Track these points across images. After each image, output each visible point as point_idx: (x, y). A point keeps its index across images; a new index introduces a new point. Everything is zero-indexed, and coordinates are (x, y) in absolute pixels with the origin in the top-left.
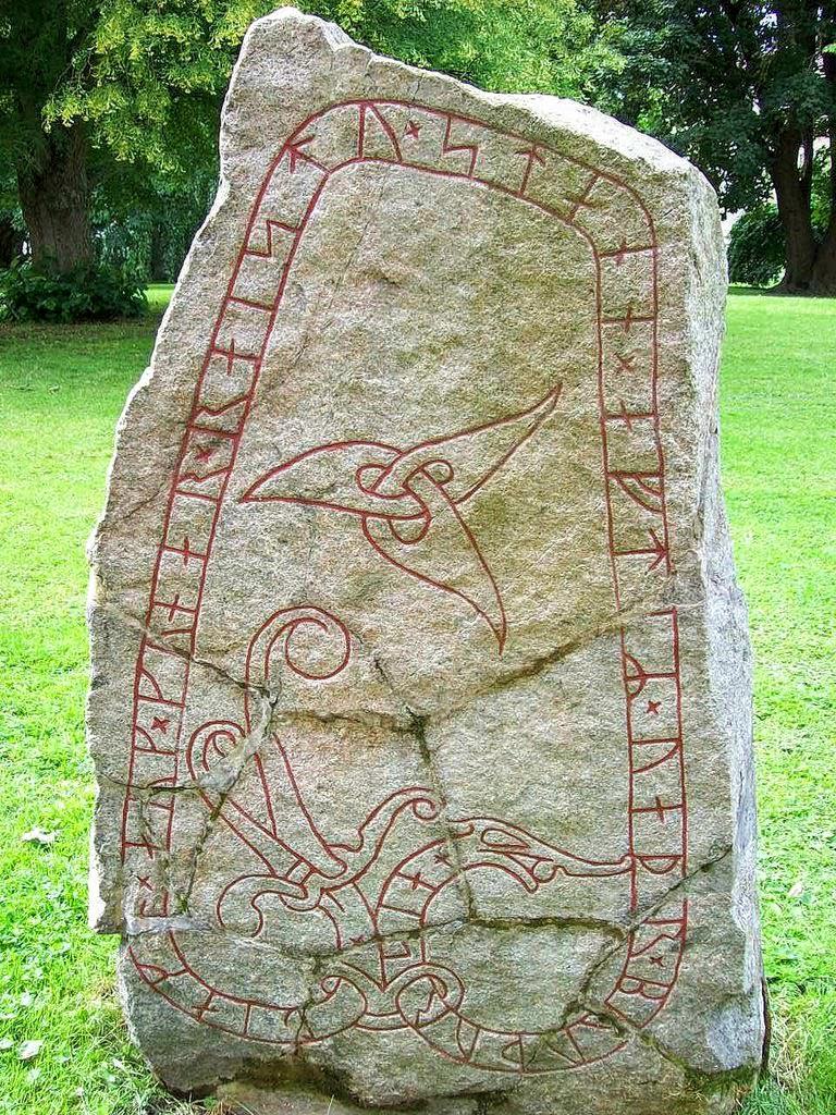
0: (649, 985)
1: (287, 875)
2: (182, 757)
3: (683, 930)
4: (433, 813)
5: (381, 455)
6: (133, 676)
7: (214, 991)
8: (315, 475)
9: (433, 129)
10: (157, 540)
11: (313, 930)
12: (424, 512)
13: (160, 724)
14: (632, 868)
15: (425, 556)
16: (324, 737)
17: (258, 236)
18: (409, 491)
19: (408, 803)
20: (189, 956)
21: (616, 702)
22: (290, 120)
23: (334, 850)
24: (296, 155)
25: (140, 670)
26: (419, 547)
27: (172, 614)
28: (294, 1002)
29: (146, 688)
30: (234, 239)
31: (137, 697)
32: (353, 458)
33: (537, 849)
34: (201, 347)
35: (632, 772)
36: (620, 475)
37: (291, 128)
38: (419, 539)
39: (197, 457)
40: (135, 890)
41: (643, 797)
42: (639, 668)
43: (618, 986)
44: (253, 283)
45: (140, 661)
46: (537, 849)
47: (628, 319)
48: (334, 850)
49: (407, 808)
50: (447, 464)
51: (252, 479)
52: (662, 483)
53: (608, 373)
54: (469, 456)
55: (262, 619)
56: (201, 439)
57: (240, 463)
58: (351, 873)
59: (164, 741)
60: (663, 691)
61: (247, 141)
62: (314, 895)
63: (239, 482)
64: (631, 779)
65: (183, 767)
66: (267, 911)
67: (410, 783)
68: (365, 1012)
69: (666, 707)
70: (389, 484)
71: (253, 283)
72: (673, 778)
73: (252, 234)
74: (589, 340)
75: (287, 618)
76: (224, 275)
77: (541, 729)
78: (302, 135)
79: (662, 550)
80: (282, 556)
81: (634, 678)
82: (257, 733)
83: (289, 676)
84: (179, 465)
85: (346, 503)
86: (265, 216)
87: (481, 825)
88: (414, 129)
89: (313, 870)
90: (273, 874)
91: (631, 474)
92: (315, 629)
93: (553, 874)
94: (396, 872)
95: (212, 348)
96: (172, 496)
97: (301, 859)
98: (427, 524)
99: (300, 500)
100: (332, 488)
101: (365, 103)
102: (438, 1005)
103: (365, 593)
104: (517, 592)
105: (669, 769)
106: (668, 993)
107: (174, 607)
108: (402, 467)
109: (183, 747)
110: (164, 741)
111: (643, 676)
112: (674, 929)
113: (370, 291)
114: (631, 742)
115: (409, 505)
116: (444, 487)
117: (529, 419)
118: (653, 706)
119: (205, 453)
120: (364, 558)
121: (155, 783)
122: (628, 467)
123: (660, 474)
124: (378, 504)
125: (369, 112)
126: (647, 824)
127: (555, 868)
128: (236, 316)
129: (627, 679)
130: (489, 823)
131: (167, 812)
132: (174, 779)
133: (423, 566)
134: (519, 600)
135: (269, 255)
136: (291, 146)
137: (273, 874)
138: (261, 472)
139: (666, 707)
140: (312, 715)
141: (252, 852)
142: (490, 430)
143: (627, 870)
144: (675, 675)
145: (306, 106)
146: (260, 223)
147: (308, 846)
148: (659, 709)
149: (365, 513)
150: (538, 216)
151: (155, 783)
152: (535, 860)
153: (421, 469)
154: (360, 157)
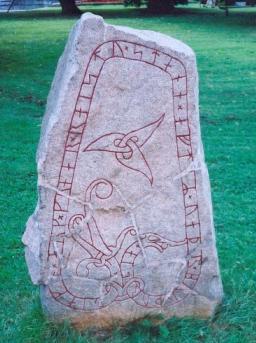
1: (98, 258)
5: (120, 136)
7: (75, 297)
8: (103, 143)
9: (131, 48)
11: (104, 271)
12: (131, 150)
13: (61, 217)
16: (106, 215)
17: (87, 79)
18: (127, 145)
21: (180, 197)
22: (95, 47)
24: (96, 56)
25: (55, 202)
29: (57, 207)
30: (80, 81)
32: (112, 138)
34: (72, 110)
36: (179, 136)
40: (52, 269)
41: (189, 223)
44: (86, 91)
47: (180, 95)
53: (176, 110)
54: (142, 135)
56: (72, 136)
57: (83, 141)
59: (61, 222)
60: (192, 192)
62: (104, 261)
63: (83, 147)
70: (123, 144)
72: (196, 216)
74: (171, 101)
76: (78, 90)
77: (162, 206)
79: (191, 155)
80: (94, 165)
82: (88, 217)
83: (96, 199)
88: (127, 48)
90: (92, 257)
95: (75, 110)
99: (100, 150)
101: (114, 41)
103: (116, 173)
105: (195, 214)
107: (65, 183)
108: (125, 140)
110: (61, 222)
111: (187, 189)
112: (199, 259)
113: (116, 92)
115: (127, 149)
119: (73, 139)
120: (117, 165)
124: (120, 150)
126: (190, 229)
133: (131, 165)
136: (95, 54)
140: (102, 210)
145: (99, 43)
154: (113, 56)
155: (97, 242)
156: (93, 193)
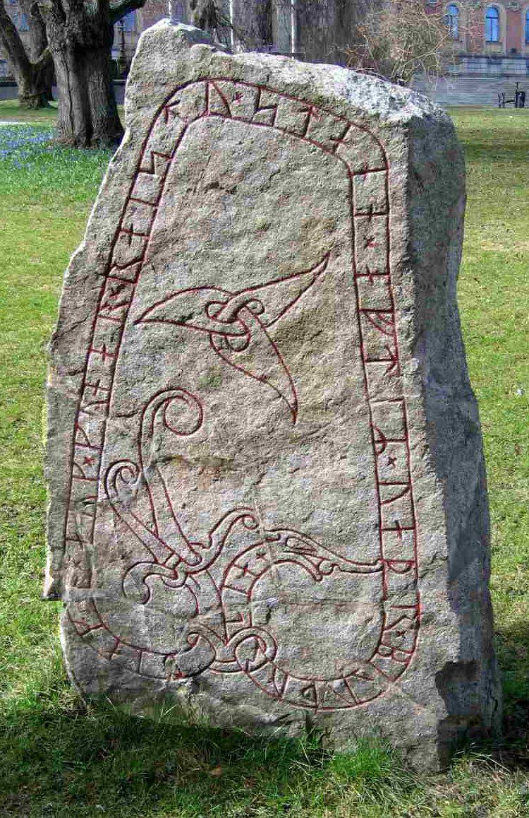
0: (397, 652)
2: (100, 483)
3: (417, 614)
4: (255, 525)
5: (221, 297)
6: (72, 430)
10: (87, 346)
12: (246, 331)
14: (382, 568)
15: (249, 359)
19: (238, 518)
20: (104, 615)
23: (194, 547)
25: (76, 427)
26: (245, 353)
27: (96, 391)
28: (169, 650)
29: (80, 438)
30: (132, 165)
31: (74, 443)
32: (206, 295)
33: (321, 552)
34: (112, 229)
35: (380, 504)
36: (365, 311)
37: (166, 95)
38: (244, 349)
39: (111, 295)
40: (71, 570)
41: (388, 521)
42: (381, 435)
43: (376, 651)
44: (144, 189)
45: (76, 420)
46: (321, 552)
48: (194, 547)
49: (239, 521)
50: (214, 302)
51: (144, 309)
52: (393, 317)
55: (149, 395)
57: (136, 300)
58: (203, 564)
61: (140, 104)
62: (181, 576)
64: (379, 509)
65: (101, 489)
66: (152, 586)
67: (241, 504)
68: (214, 659)
69: (401, 461)
71: (144, 189)
73: (143, 161)
75: (165, 395)
76: (127, 184)
78: (173, 100)
81: (378, 442)
84: (100, 300)
85: (201, 325)
86: (151, 149)
87: (285, 534)
88: (238, 96)
89: (181, 560)
91: (373, 311)
92: (181, 403)
93: (332, 570)
94: (232, 563)
95: (119, 229)
96: (96, 318)
97: (173, 552)
98: (248, 340)
100: (190, 317)
102: (260, 657)
104: (305, 383)
106: (410, 657)
109: (102, 475)
112: (411, 612)
114: (378, 484)
116: (259, 316)
117: (307, 277)
118: (391, 461)
119: (115, 293)
121: (84, 499)
122: (372, 306)
123: (392, 311)
124: (218, 326)
125: (211, 87)
126: (390, 540)
127: (333, 565)
128: (134, 209)
129: (374, 442)
130: (290, 533)
131: (91, 518)
132: (96, 497)
133: (247, 365)
134: (306, 389)
135: (153, 173)
137: (156, 562)
138: (149, 305)
139: (401, 461)
141: (143, 547)
142: (272, 286)
143: (377, 571)
144: (406, 440)
146: (147, 153)
147: (174, 543)
148: (395, 463)
149: (211, 332)
150: (315, 150)
151: (84, 499)
152: (320, 560)
153: (244, 304)
155: (167, 528)
156: (158, 419)
